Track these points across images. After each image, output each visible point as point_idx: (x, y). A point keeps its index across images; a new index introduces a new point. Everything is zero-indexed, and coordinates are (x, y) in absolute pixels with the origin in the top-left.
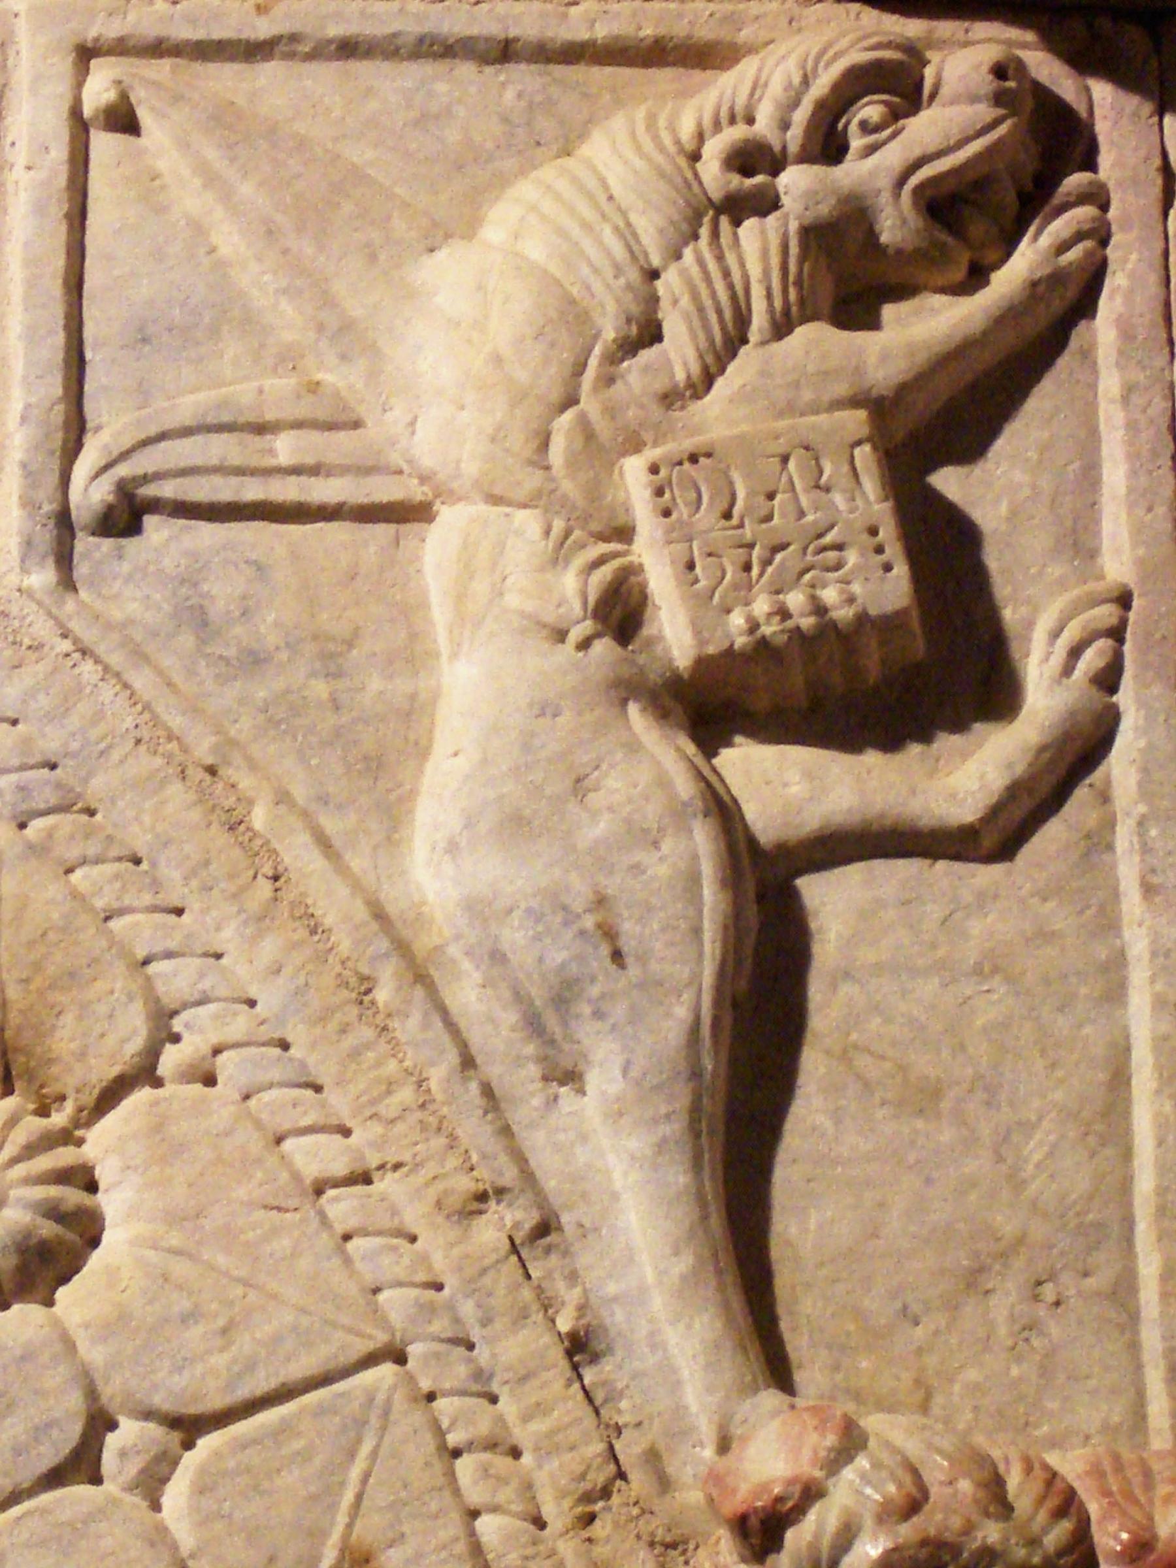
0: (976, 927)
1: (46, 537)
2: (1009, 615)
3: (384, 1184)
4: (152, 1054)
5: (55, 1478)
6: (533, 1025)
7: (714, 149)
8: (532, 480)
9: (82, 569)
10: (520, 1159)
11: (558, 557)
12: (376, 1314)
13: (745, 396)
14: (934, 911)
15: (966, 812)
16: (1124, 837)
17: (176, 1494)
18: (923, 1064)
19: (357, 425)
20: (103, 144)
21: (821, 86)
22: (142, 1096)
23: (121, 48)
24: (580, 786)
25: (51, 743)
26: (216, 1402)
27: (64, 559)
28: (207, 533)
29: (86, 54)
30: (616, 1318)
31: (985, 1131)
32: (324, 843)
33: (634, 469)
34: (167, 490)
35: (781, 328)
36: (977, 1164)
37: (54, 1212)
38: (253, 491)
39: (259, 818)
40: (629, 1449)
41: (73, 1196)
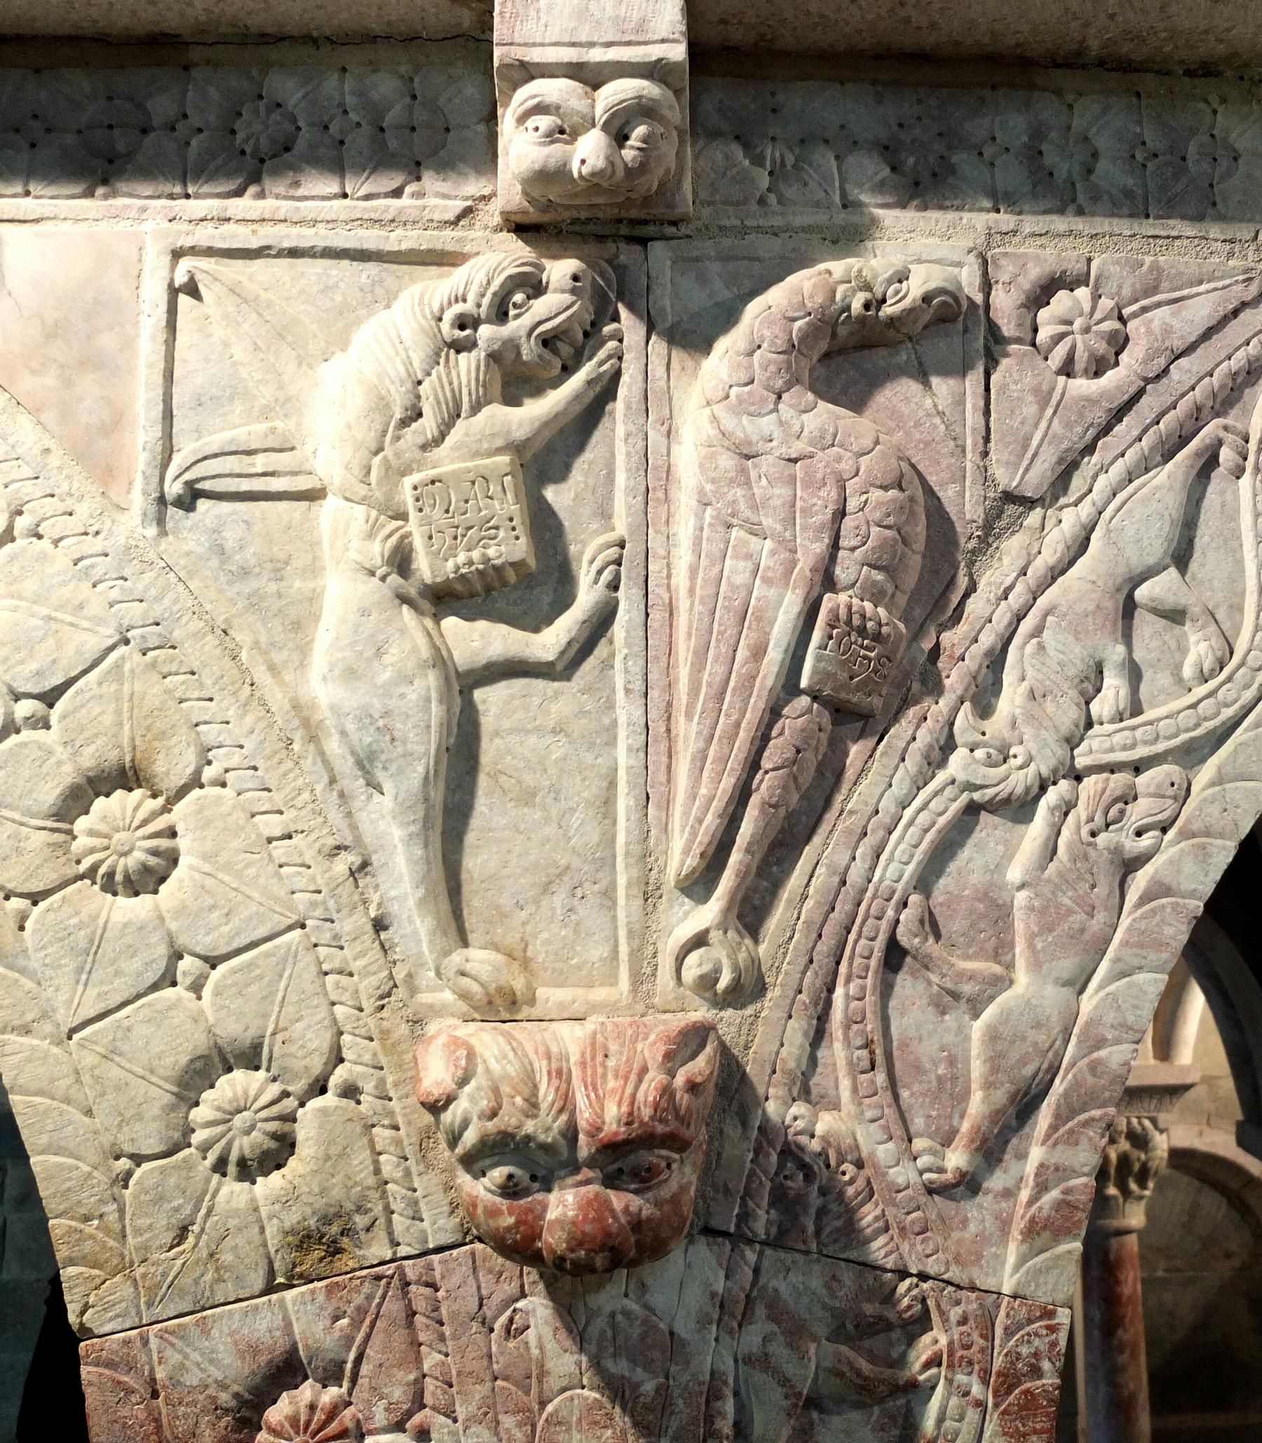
0: (553, 708)
1: (153, 509)
2: (573, 549)
3: (297, 839)
4: (198, 773)
5: (155, 987)
6: (360, 764)
7: (449, 316)
8: (362, 490)
9: (169, 525)
10: (354, 827)
11: (371, 535)
12: (291, 908)
13: (453, 448)
14: (536, 701)
15: (549, 655)
16: (618, 659)
17: (207, 992)
18: (529, 779)
19: (292, 449)
20: (184, 300)
21: (495, 286)
22: (196, 792)
23: (194, 251)
24: (379, 652)
25: (157, 611)
26: (223, 950)
27: (161, 521)
28: (225, 507)
29: (177, 254)
30: (394, 908)
31: (554, 812)
32: (272, 668)
33: (408, 481)
34: (206, 485)
35: (476, 409)
36: (549, 830)
37: (155, 852)
38: (245, 485)
39: (244, 656)
40: (400, 975)
41: (164, 843)
